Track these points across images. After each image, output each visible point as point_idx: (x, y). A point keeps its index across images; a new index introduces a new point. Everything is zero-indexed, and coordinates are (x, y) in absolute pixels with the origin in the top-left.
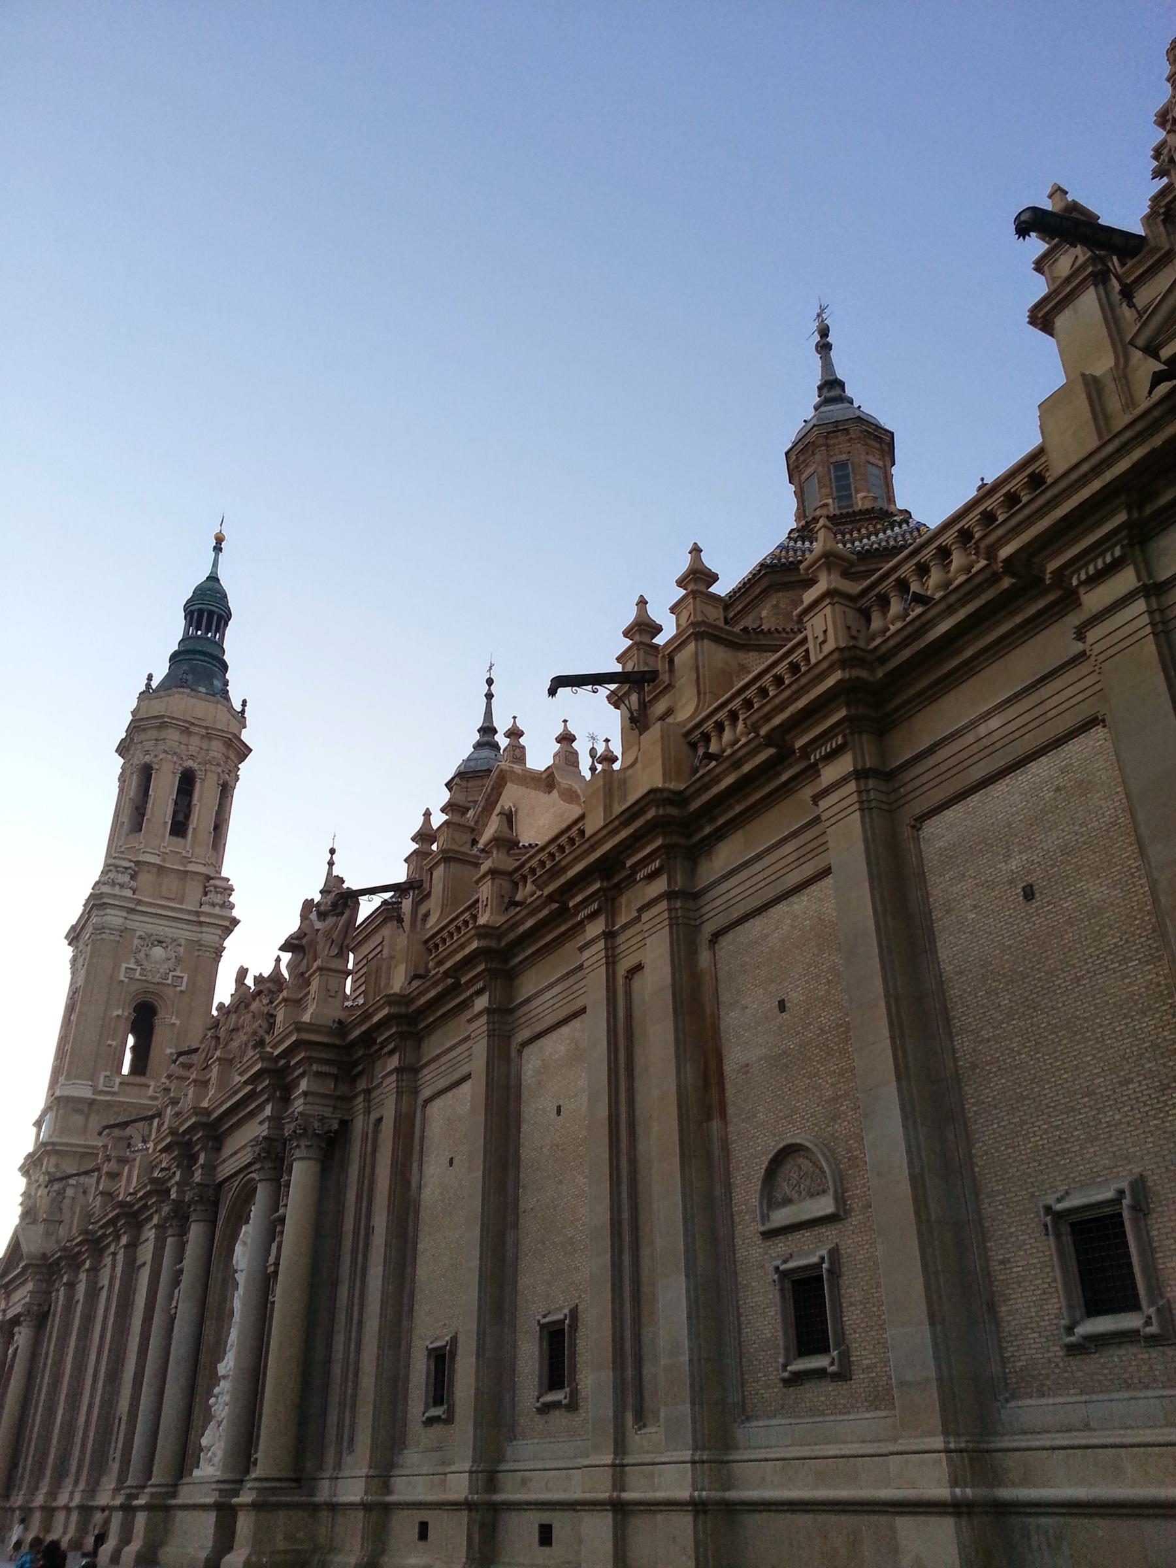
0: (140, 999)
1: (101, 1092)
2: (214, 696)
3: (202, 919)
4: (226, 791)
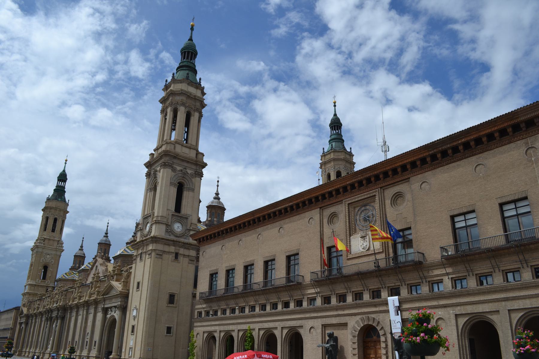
0: (44, 265)
1: (37, 283)
2: (62, 201)
3: (57, 250)
4: (63, 222)
